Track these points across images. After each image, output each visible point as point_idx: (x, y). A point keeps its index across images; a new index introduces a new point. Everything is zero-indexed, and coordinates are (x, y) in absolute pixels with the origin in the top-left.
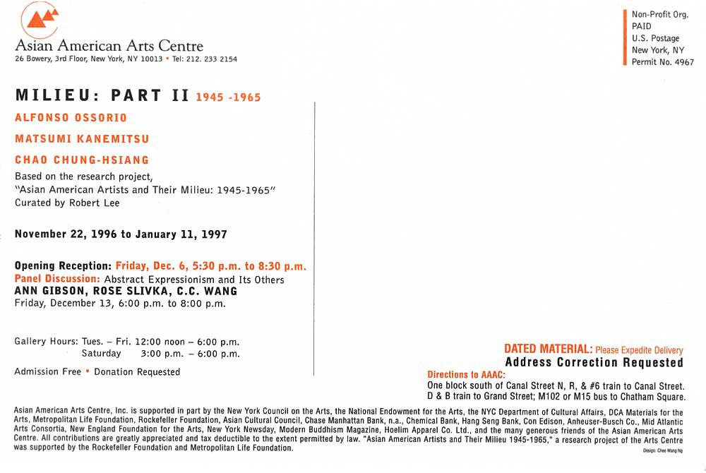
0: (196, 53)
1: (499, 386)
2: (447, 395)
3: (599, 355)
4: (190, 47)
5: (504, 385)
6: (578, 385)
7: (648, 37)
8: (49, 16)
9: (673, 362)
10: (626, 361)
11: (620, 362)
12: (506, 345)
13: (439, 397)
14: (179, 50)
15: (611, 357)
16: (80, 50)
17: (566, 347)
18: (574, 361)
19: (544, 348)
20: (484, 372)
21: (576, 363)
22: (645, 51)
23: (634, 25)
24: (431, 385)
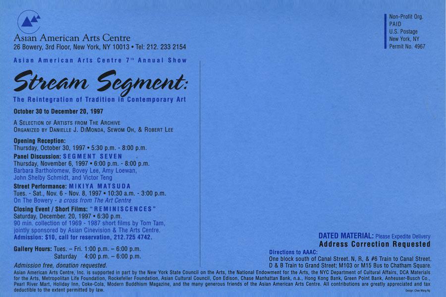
0: (126, 43)
1: (314, 259)
2: (282, 265)
3: (378, 239)
4: (122, 39)
5: (317, 259)
6: (364, 258)
7: (399, 31)
8: (34, 20)
9: (424, 244)
10: (394, 243)
11: (391, 244)
12: (320, 233)
13: (276, 266)
14: (115, 40)
15: (385, 241)
16: (54, 40)
17: (357, 234)
18: (362, 243)
19: (343, 235)
20: (304, 250)
21: (363, 244)
22: (397, 39)
23: (391, 23)
24: (271, 259)
